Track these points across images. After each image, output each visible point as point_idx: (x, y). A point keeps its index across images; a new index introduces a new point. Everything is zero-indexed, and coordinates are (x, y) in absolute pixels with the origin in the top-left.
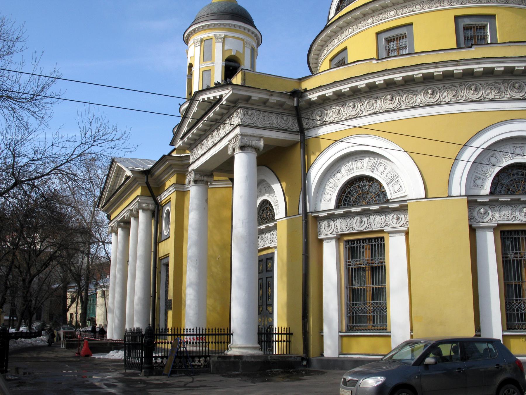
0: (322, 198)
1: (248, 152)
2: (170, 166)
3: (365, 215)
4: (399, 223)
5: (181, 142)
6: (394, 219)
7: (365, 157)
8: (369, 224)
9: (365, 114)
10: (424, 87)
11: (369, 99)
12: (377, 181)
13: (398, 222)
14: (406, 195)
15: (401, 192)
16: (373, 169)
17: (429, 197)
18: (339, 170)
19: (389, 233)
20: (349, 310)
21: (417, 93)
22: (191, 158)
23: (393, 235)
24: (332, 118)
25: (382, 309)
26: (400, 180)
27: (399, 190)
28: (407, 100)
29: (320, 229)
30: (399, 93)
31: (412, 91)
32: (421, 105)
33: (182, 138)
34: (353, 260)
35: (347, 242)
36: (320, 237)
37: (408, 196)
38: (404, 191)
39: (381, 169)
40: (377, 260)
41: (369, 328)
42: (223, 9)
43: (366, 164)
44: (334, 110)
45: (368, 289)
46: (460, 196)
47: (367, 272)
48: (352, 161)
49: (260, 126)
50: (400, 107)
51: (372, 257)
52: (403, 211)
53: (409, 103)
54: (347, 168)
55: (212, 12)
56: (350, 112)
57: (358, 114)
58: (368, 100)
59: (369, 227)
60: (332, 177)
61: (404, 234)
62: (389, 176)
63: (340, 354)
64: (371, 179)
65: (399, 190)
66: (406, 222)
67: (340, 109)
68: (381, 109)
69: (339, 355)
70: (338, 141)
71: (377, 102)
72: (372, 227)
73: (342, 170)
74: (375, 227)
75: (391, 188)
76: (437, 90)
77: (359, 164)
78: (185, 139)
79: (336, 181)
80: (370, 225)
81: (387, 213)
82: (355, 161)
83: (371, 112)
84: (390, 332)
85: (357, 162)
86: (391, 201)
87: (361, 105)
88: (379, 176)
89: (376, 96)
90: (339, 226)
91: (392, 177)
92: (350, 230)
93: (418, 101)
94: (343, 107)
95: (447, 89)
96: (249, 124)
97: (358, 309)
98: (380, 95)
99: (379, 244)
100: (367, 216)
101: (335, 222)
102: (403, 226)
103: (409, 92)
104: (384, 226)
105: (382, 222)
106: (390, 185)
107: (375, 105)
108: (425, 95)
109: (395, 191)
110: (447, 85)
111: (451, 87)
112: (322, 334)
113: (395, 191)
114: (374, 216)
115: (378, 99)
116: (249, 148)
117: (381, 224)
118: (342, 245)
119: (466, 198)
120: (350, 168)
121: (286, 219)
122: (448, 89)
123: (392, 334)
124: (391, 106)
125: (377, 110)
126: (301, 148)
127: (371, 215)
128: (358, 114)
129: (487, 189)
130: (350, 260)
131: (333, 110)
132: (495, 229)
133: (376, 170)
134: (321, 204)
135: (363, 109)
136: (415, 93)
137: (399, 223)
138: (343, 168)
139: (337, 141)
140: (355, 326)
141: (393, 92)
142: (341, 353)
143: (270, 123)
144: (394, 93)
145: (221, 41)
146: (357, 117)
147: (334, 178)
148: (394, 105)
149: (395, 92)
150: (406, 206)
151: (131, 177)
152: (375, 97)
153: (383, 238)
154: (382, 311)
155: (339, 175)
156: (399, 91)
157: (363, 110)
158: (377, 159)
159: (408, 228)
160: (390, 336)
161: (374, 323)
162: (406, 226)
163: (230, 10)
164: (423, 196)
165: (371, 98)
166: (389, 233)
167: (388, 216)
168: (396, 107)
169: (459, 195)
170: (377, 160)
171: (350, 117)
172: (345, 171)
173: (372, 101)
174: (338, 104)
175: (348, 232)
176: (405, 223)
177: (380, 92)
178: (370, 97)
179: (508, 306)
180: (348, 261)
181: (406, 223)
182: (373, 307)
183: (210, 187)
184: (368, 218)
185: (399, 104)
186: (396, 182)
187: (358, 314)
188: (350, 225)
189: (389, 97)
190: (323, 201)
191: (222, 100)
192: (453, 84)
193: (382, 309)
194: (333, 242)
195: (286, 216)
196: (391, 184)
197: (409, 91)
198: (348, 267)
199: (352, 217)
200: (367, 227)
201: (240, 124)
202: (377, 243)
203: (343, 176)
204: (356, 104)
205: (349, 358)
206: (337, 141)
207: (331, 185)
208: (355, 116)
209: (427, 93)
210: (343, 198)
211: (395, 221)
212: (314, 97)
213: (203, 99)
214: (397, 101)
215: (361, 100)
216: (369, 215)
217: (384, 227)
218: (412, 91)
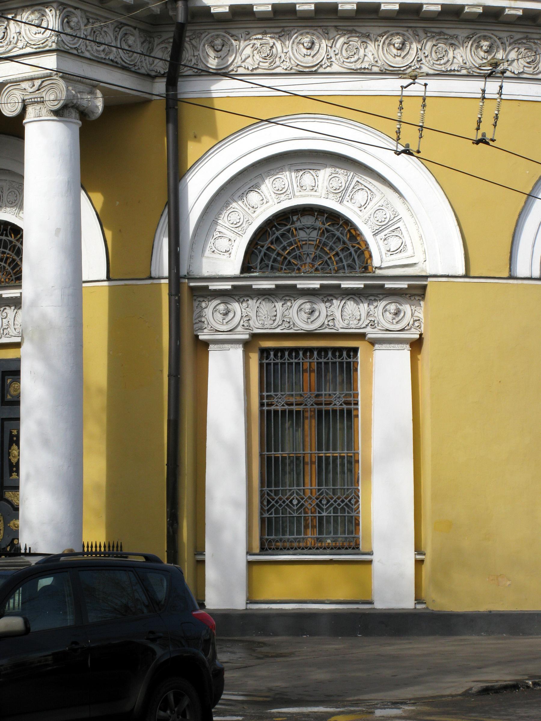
0: (207, 245)
1: (70, 120)
3: (321, 297)
4: (397, 322)
6: (387, 313)
7: (325, 166)
8: (329, 318)
9: (335, 68)
10: (473, 31)
11: (349, 35)
12: (347, 222)
13: (397, 319)
14: (415, 264)
15: (403, 255)
17: (472, 274)
18: (255, 187)
19: (373, 342)
20: (265, 503)
21: (456, 43)
23: (384, 346)
24: (249, 60)
25: (346, 505)
27: (399, 250)
28: (433, 53)
29: (202, 316)
30: (418, 35)
31: (446, 37)
32: (464, 72)
34: (279, 393)
35: (264, 352)
36: (202, 337)
37: (420, 265)
38: (409, 252)
39: (361, 197)
40: (339, 398)
41: (309, 544)
43: (326, 184)
44: (258, 43)
45: (308, 459)
46: (531, 278)
47: (307, 422)
48: (290, 171)
49: (87, 55)
50: (420, 68)
51: (318, 390)
52: (408, 296)
53: (438, 62)
54: (278, 184)
56: (300, 57)
57: (321, 66)
58: (347, 36)
59: (331, 323)
60: (236, 198)
61: (408, 346)
62: (380, 215)
63: (251, 603)
65: (399, 250)
66: (415, 321)
67: (274, 44)
68: (375, 64)
69: (247, 603)
70: (266, 121)
71: (366, 47)
72: (337, 325)
73: (263, 187)
74: (345, 325)
75: (381, 243)
76: (499, 42)
77: (307, 179)
79: (247, 209)
80: (333, 319)
81: (373, 298)
82: (298, 171)
83: (353, 66)
84: (371, 553)
85: (301, 173)
86: (378, 272)
87: (330, 45)
88: (355, 212)
89: (364, 30)
90: (253, 315)
91: (387, 220)
92: (280, 328)
93: (459, 60)
94: (280, 40)
95: (517, 45)
96: (71, 48)
97: (291, 502)
98: (375, 31)
99: (343, 363)
100: (325, 299)
101: (245, 304)
102: (407, 330)
103: (440, 36)
104: (364, 325)
105: (360, 315)
106: (378, 237)
107: (362, 52)
108: (473, 49)
109: (389, 251)
110: (518, 36)
111: (525, 41)
112: (199, 558)
113: (389, 251)
114: (343, 302)
115: (371, 40)
116: (72, 110)
117: (359, 320)
118: (255, 358)
120: (286, 186)
121: (106, 283)
122: (520, 46)
123: (375, 558)
124: (399, 62)
125: (365, 65)
126: (168, 122)
127: (337, 299)
128: (320, 65)
130: (272, 393)
131: (253, 42)
133: (349, 199)
134: (204, 260)
135: (332, 54)
136: (453, 42)
137: (397, 322)
138: (268, 182)
139: (262, 121)
140: (274, 540)
141: (406, 29)
142: (250, 601)
143: (103, 50)
144: (409, 34)
146: (315, 73)
147: (240, 203)
148: (407, 62)
149: (410, 31)
150: (424, 287)
152: (362, 34)
153: (355, 350)
154: (347, 509)
155: (253, 197)
156: (417, 29)
157: (333, 59)
158: (352, 174)
159: (421, 335)
160: (370, 562)
161: (320, 533)
162: (413, 330)
164: (461, 271)
165: (353, 35)
166: (373, 342)
167: (375, 304)
168: (410, 67)
169: (528, 275)
170: (353, 178)
171: (301, 69)
172: (271, 190)
173: (355, 42)
174: (268, 30)
175: (278, 331)
176: (411, 323)
177: (376, 24)
178: (351, 32)
180: (265, 394)
181: (413, 324)
182: (298, 500)
184: (328, 304)
185: (418, 61)
186: (393, 231)
187: (290, 513)
188: (283, 316)
189: (397, 40)
190: (207, 253)
192: (530, 36)
193: (346, 505)
194: (238, 352)
195: (109, 279)
196: (382, 235)
197: (440, 34)
198: (265, 408)
199: (287, 298)
200: (326, 323)
202: (340, 360)
203: (265, 201)
204: (316, 41)
205: (271, 609)
206: (262, 121)
207: (234, 217)
208: (314, 69)
209: (479, 47)
210: (260, 252)
211: (389, 316)
214: (413, 52)
215: (327, 34)
216: (330, 298)
217: (364, 328)
218: (446, 37)
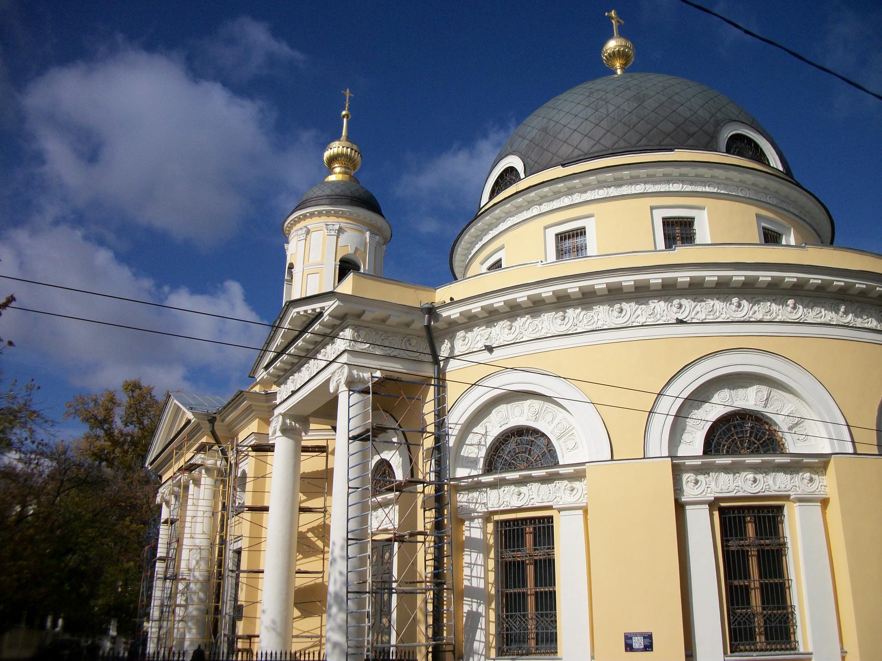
2: (249, 409)
5: (265, 373)
13: (573, 494)
16: (537, 416)
22: (278, 396)
26: (575, 433)
33: (267, 368)
39: (549, 417)
42: (339, 190)
64: (535, 432)
68: (549, 331)
78: (271, 370)
106: (561, 441)
119: (670, 459)
129: (698, 448)
132: (713, 504)
145: (334, 234)
148: (568, 327)
150: (584, 471)
151: (192, 422)
153: (550, 519)
163: (349, 191)
164: (610, 458)
168: (570, 330)
175: (501, 508)
179: (732, 618)
183: (304, 438)
191: (323, 315)
196: (563, 439)
201: (349, 349)
212: (453, 313)
213: (298, 313)
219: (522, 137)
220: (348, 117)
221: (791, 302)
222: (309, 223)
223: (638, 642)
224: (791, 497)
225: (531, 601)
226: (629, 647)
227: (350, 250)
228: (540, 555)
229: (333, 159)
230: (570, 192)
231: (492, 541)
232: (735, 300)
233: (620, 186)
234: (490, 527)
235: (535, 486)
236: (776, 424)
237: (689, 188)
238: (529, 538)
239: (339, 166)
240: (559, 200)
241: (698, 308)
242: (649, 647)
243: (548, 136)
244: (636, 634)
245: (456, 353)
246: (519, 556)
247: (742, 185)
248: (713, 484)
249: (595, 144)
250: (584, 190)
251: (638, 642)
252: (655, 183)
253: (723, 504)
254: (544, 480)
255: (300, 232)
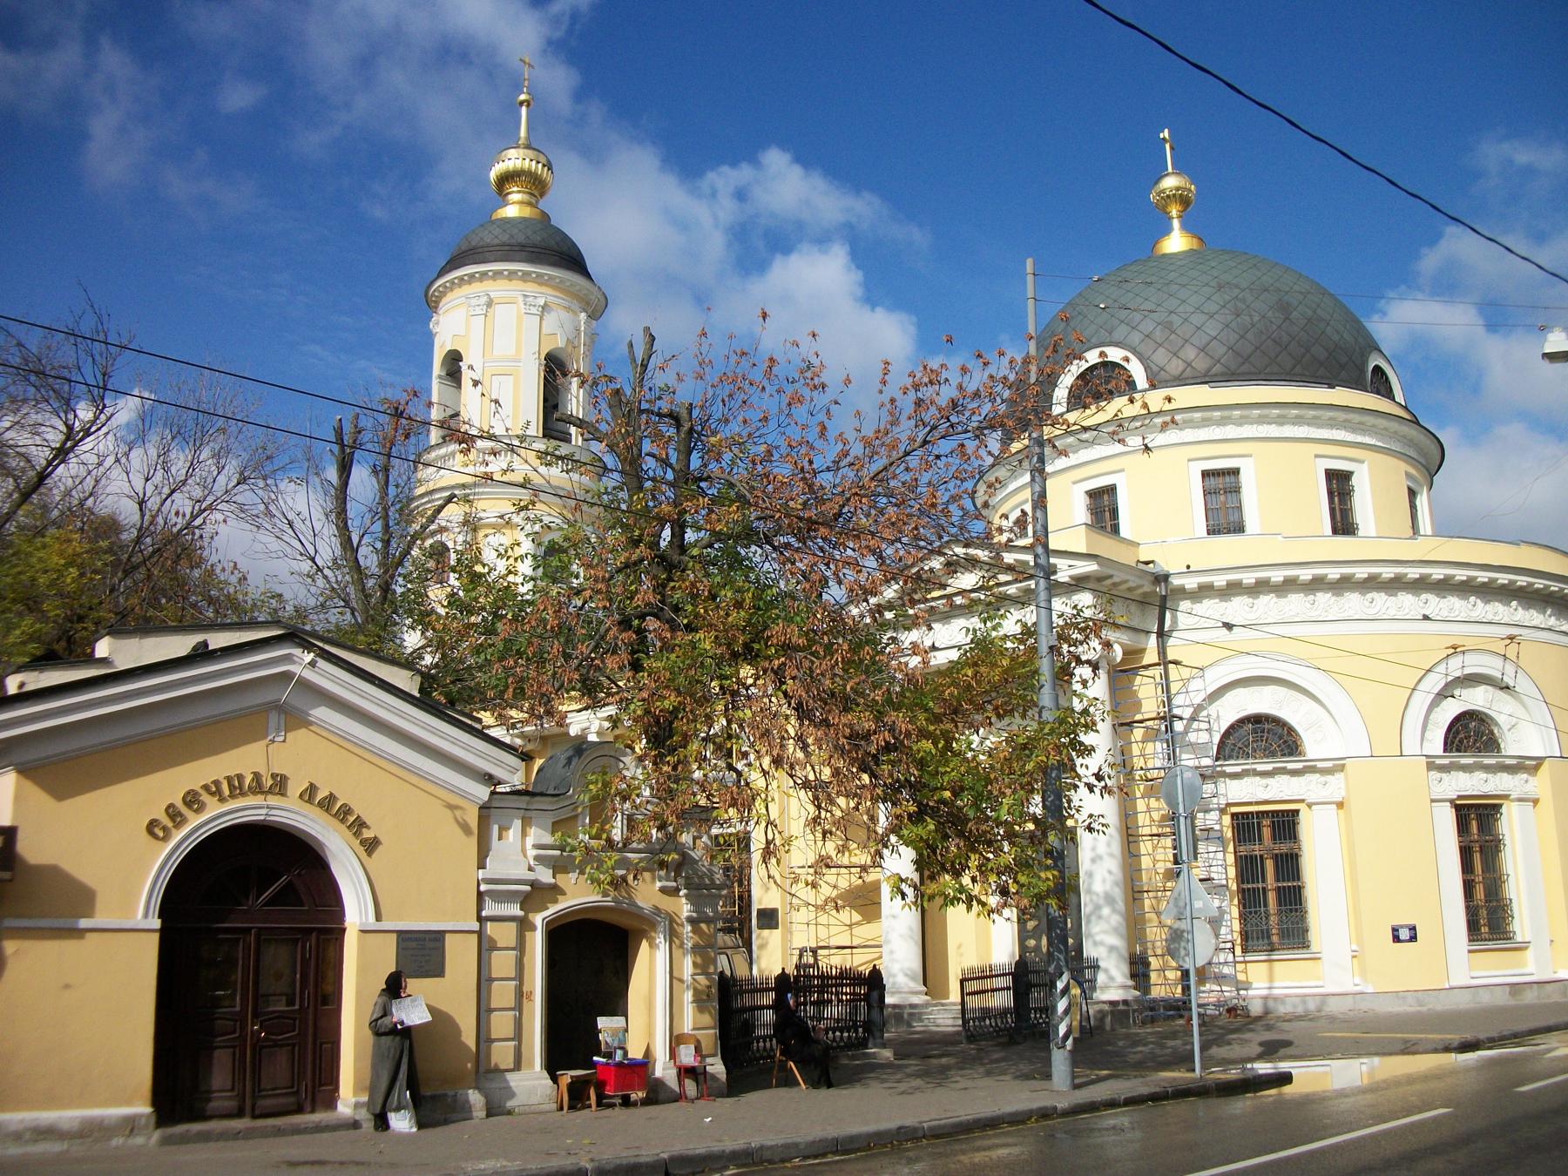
35: (1233, 815)
42: (539, 239)
55: (513, 241)
148: (1317, 613)
166: (1310, 806)
212: (1191, 583)
219: (1127, 325)
220: (528, 106)
221: (1514, 603)
222: (497, 289)
223: (1404, 934)
224: (1512, 797)
225: (1272, 896)
226: (1396, 939)
227: (560, 342)
228: (1284, 848)
229: (506, 179)
230: (1222, 422)
231: (1229, 835)
232: (1472, 599)
233: (1281, 424)
234: (1227, 820)
235: (1286, 778)
236: (1497, 724)
237: (1350, 437)
238: (1267, 832)
239: (519, 192)
240: (1206, 429)
241: (1441, 605)
242: (1413, 938)
243: (1173, 336)
244: (1402, 927)
245: (1181, 626)
246: (1256, 849)
247: (1394, 436)
248: (1453, 783)
249: (1243, 363)
250: (1240, 422)
251: (1404, 934)
252: (1319, 426)
253: (1458, 802)
254: (1294, 773)
255: (474, 302)
